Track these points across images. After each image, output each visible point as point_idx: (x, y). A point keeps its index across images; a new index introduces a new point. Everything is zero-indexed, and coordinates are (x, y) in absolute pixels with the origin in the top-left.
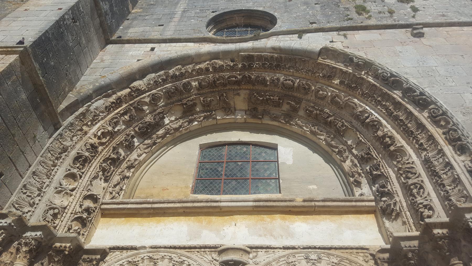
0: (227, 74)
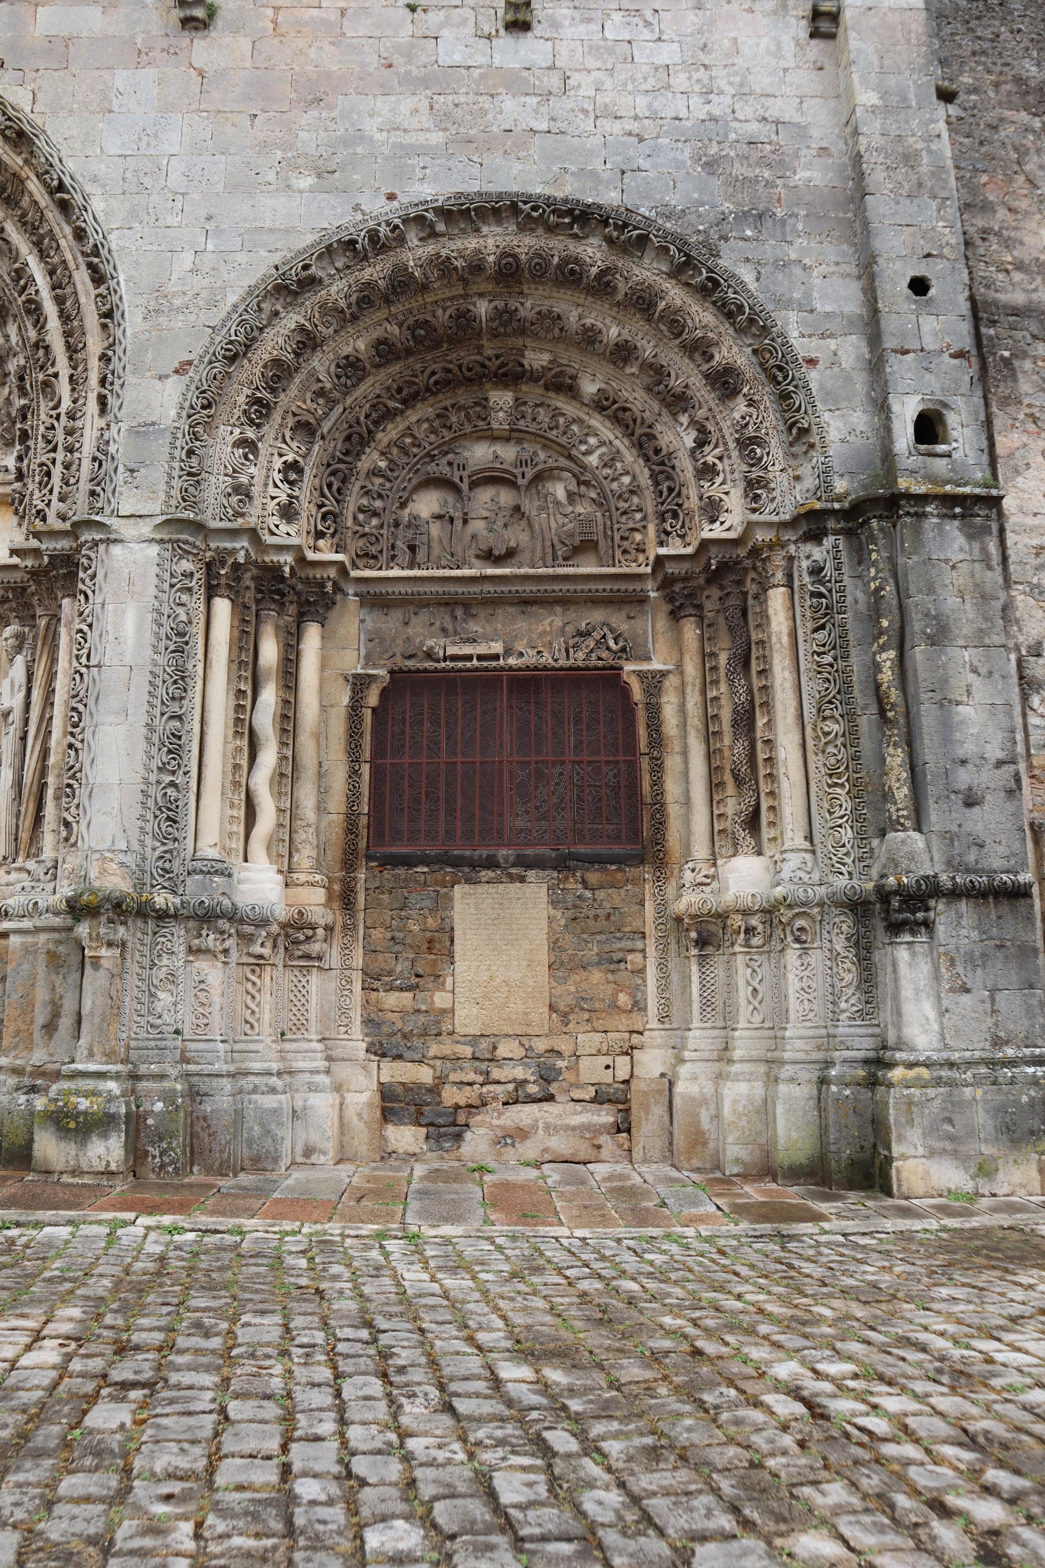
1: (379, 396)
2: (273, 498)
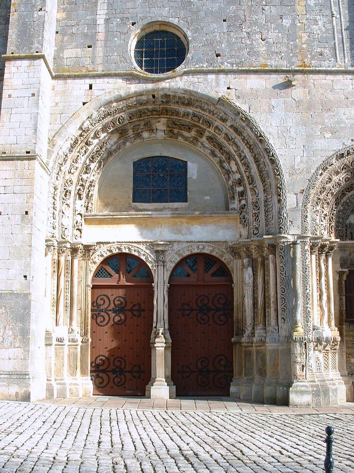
0: (150, 107)
1: (343, 191)
2: (322, 225)
